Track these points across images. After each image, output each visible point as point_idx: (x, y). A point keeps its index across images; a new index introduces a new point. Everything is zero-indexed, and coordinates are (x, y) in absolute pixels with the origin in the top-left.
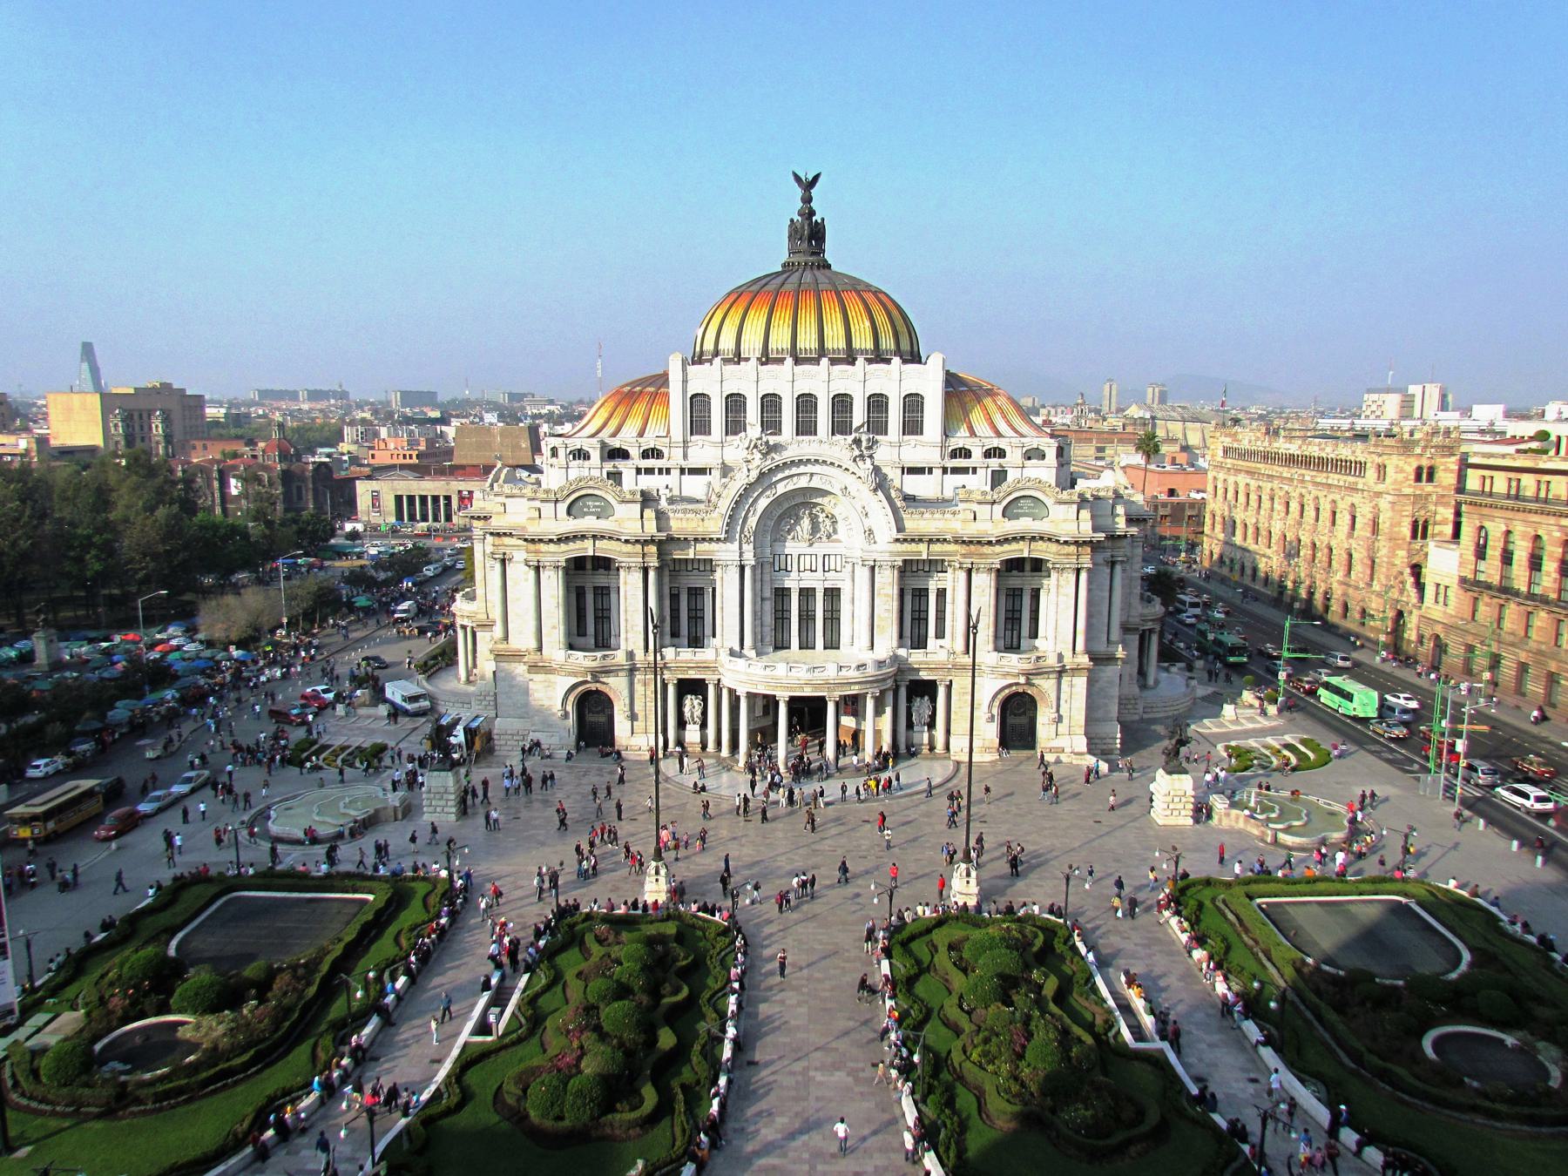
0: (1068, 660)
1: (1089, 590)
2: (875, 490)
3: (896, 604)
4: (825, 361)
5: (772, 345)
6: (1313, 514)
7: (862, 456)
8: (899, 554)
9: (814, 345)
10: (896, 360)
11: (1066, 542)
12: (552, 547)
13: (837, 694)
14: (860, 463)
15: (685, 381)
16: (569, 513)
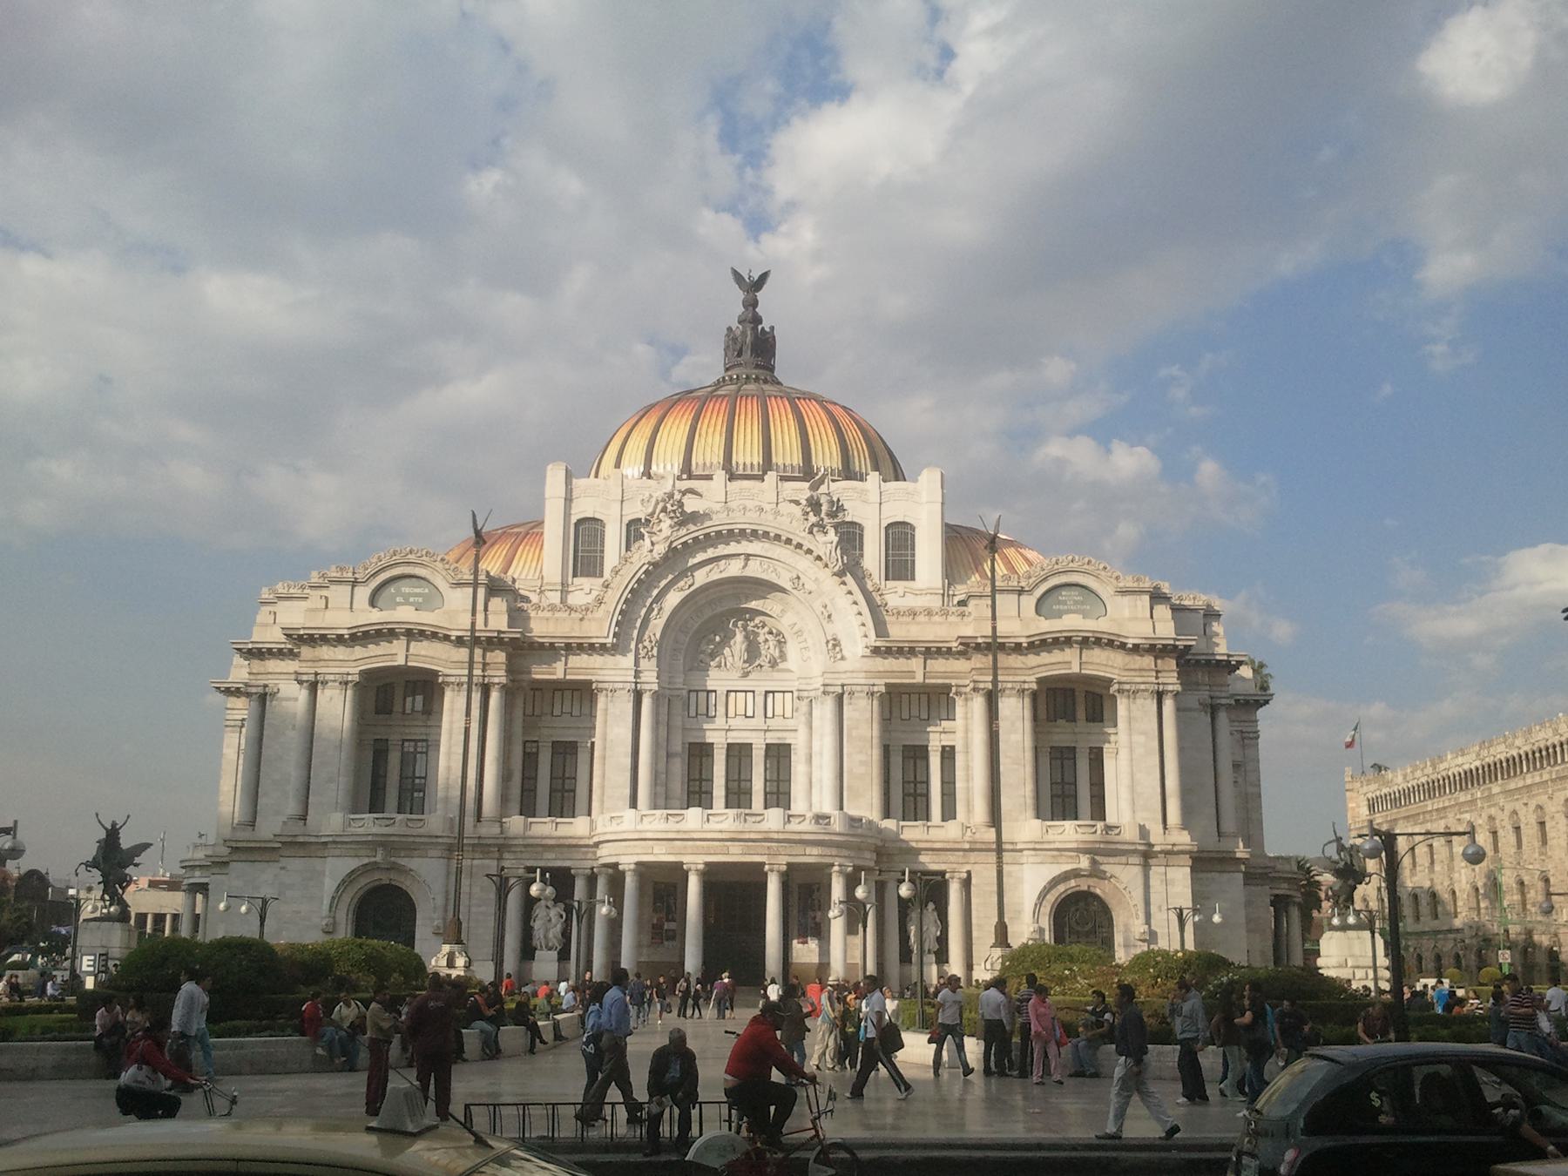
0: (1157, 837)
1: (1182, 750)
2: (840, 574)
3: (876, 754)
4: (771, 477)
5: (696, 459)
6: (1512, 839)
7: (821, 527)
8: (880, 675)
9: (757, 459)
10: (874, 477)
11: (1136, 649)
12: (341, 652)
13: (784, 860)
14: (820, 537)
15: (569, 500)
16: (373, 602)
